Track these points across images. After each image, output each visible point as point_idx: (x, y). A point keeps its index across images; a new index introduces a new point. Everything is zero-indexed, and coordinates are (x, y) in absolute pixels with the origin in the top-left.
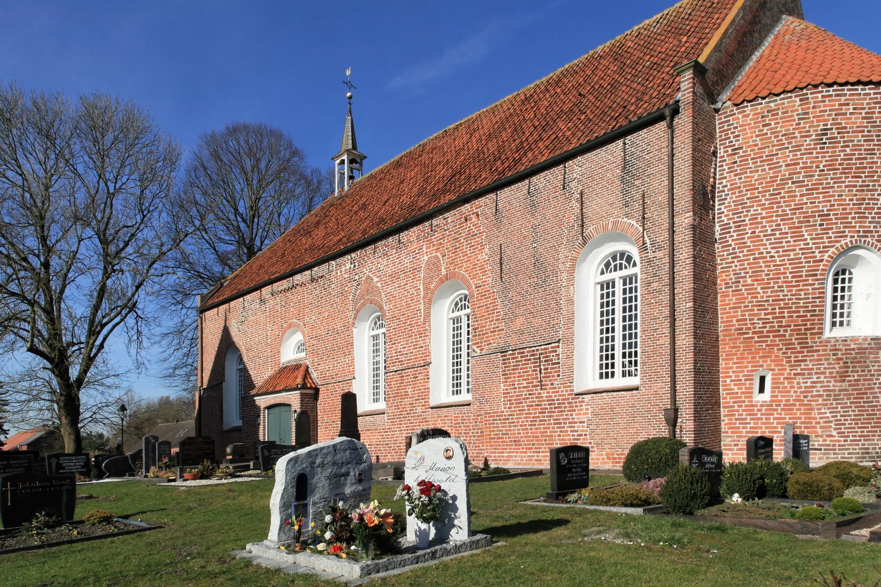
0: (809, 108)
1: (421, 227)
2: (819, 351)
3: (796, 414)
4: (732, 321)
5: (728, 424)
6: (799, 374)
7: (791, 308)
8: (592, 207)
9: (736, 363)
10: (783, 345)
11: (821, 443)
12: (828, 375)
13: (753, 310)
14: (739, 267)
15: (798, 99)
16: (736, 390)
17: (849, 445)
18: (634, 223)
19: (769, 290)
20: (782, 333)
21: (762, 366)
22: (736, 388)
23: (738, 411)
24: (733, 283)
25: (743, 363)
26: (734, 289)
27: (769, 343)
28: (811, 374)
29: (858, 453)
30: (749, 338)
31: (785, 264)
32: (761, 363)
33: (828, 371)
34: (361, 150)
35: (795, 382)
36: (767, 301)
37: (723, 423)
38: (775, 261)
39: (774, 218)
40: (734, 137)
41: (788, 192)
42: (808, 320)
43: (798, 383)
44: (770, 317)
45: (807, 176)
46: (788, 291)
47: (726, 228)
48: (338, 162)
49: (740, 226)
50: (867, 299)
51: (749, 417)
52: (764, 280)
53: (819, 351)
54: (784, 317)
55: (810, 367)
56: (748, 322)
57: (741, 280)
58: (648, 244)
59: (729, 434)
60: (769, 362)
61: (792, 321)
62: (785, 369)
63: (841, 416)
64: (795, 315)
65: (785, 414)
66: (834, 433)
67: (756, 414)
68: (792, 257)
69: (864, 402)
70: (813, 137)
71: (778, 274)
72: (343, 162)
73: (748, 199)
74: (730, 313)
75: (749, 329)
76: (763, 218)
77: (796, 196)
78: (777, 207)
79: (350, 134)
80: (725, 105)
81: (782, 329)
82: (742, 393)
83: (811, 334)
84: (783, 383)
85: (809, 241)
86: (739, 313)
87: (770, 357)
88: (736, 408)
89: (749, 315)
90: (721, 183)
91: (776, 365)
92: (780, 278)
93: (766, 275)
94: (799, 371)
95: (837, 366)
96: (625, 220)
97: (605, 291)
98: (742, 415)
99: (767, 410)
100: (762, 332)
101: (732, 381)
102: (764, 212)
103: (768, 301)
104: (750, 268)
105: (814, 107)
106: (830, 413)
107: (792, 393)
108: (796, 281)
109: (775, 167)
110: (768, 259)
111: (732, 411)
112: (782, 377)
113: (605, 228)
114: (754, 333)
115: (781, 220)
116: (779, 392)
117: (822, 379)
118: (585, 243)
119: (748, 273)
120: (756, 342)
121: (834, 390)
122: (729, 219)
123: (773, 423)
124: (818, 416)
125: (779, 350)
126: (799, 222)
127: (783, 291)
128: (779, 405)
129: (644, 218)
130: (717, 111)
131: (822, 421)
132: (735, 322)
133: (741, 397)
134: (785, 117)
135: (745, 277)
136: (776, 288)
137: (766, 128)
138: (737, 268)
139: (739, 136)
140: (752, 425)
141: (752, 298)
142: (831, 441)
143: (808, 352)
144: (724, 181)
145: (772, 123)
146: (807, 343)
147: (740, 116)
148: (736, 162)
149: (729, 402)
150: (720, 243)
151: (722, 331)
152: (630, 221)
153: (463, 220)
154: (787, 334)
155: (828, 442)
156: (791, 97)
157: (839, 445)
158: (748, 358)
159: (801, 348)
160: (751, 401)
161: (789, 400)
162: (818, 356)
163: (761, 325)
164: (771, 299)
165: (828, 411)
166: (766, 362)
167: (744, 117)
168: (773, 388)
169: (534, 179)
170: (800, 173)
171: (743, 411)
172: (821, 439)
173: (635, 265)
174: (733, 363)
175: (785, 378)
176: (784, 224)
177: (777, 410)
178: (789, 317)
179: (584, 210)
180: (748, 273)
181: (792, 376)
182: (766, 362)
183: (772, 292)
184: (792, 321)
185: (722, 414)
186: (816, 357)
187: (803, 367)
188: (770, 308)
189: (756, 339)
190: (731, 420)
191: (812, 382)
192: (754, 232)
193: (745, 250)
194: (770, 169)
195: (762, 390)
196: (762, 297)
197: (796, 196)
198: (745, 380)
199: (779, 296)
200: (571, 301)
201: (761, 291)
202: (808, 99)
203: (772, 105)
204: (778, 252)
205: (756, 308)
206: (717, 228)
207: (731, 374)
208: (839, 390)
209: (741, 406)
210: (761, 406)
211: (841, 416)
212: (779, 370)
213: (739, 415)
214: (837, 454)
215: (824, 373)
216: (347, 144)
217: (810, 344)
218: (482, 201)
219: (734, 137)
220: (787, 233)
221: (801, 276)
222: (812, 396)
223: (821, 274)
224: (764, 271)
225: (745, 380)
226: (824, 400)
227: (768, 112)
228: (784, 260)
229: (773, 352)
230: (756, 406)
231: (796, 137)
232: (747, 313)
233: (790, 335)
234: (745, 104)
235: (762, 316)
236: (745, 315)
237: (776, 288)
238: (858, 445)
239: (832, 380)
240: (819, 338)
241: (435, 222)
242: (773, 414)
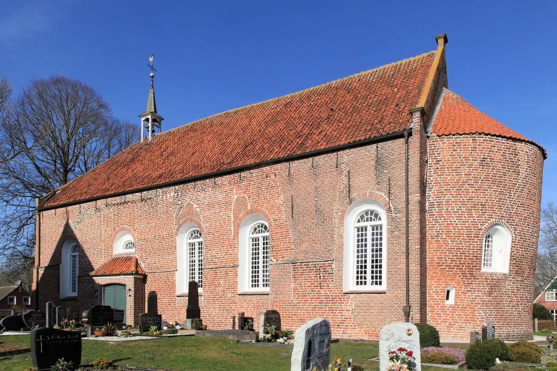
0: (476, 145)
1: (232, 176)
5: (431, 316)
6: (469, 291)
8: (355, 182)
10: (462, 274)
15: (471, 139)
18: (383, 195)
21: (450, 285)
23: (436, 309)
34: (160, 113)
37: (428, 316)
38: (458, 227)
39: (458, 203)
40: (437, 154)
41: (465, 189)
43: (469, 296)
45: (475, 182)
47: (432, 205)
48: (144, 119)
49: (440, 205)
50: (500, 252)
54: (462, 259)
58: (392, 208)
61: (466, 261)
62: (462, 288)
70: (478, 161)
72: (147, 120)
73: (444, 190)
75: (444, 263)
76: (452, 202)
77: (469, 192)
78: (460, 197)
79: (153, 101)
80: (432, 135)
82: (439, 299)
83: (476, 269)
84: (461, 295)
85: (475, 218)
90: (430, 179)
91: (458, 285)
93: (454, 234)
94: (469, 289)
96: (378, 192)
97: (360, 233)
100: (451, 266)
102: (453, 199)
105: (479, 145)
108: (469, 239)
109: (459, 174)
113: (364, 195)
114: (446, 266)
115: (462, 204)
118: (351, 202)
120: (447, 271)
122: (434, 200)
126: (471, 207)
128: (459, 307)
129: (390, 193)
130: (428, 137)
132: (436, 259)
133: (438, 302)
134: (465, 148)
137: (455, 152)
139: (440, 154)
143: (474, 279)
144: (431, 178)
145: (458, 150)
147: (441, 143)
148: (438, 168)
150: (429, 213)
151: (429, 263)
152: (381, 193)
153: (264, 176)
156: (468, 137)
158: (442, 280)
161: (463, 305)
167: (443, 143)
169: (316, 158)
170: (472, 180)
171: (439, 309)
173: (380, 219)
176: (463, 207)
179: (351, 183)
184: (466, 261)
185: (428, 310)
189: (447, 269)
190: (432, 314)
192: (447, 209)
193: (442, 218)
194: (456, 175)
196: (451, 246)
197: (469, 192)
200: (341, 237)
202: (476, 140)
203: (458, 139)
204: (460, 222)
206: (427, 204)
209: (438, 307)
210: (450, 307)
216: (150, 108)
218: (279, 166)
219: (437, 154)
220: (465, 212)
221: (471, 237)
223: (481, 237)
227: (456, 143)
231: (470, 160)
233: (465, 269)
234: (444, 136)
235: (451, 257)
241: (243, 174)
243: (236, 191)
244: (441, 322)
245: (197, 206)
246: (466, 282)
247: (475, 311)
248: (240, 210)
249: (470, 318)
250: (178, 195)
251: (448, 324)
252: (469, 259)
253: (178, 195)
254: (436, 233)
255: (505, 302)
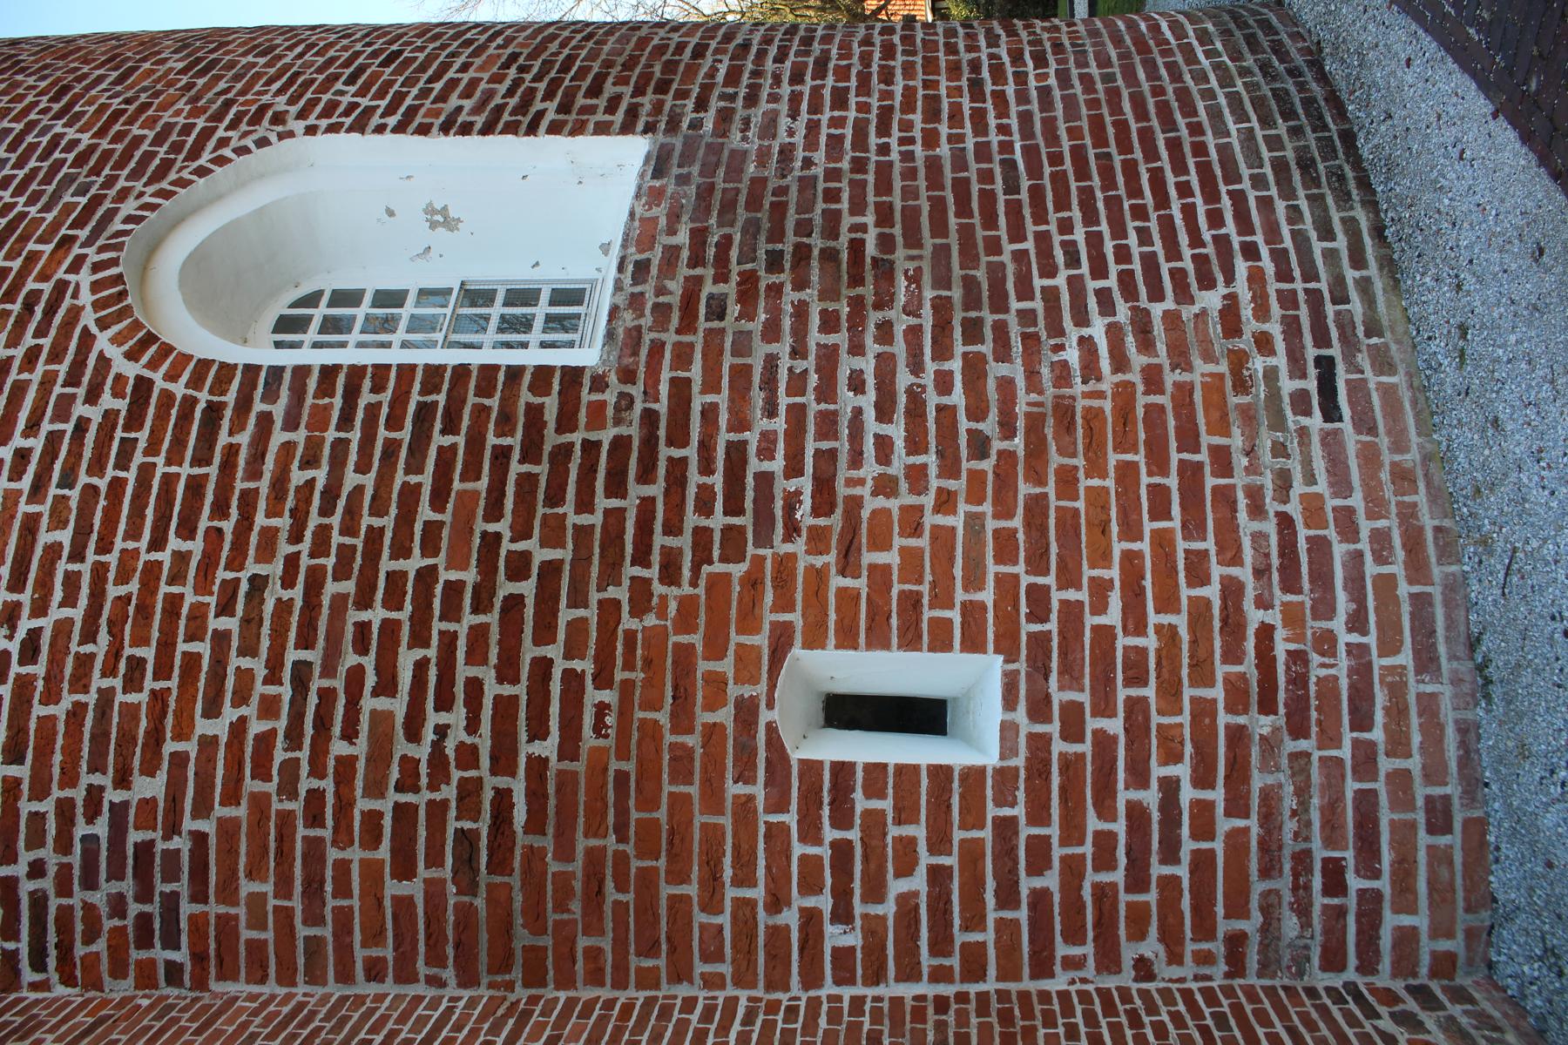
2: (681, 388)
3: (1097, 499)
4: (404, 905)
7: (375, 535)
9: (712, 883)
10: (611, 574)
11: (1281, 361)
12: (841, 338)
13: (346, 766)
14: (47, 853)
16: (918, 882)
17: (1273, 234)
19: (235, 662)
20: (527, 588)
21: (747, 712)
22: (897, 887)
23: (1072, 869)
24: (144, 895)
25: (713, 836)
26: (183, 886)
27: (585, 666)
28: (828, 424)
29: (1316, 200)
30: (536, 795)
31: (99, 571)
32: (725, 716)
33: (815, 337)
35: (871, 504)
36: (301, 674)
38: (63, 627)
42: (475, 442)
43: (885, 486)
44: (406, 660)
46: (267, 550)
51: (1123, 796)
52: (158, 697)
53: (681, 388)
54: (427, 576)
55: (780, 424)
56: (421, 799)
57: (134, 837)
59: (1251, 925)
60: (727, 666)
62: (785, 565)
63: (1099, 271)
64: (425, 513)
65: (1102, 557)
66: (1212, 300)
67: (1104, 743)
68: (65, 537)
69: (1012, 187)
71: (144, 611)
74: (343, 920)
75: (470, 791)
81: (505, 588)
82: (939, 842)
83: (566, 422)
84: (880, 576)
86: (355, 854)
87: (685, 656)
88: (1051, 880)
89: (376, 788)
91: (749, 622)
92: (174, 602)
94: (805, 484)
95: (790, 296)
98: (1105, 842)
99: (1070, 675)
100: (505, 706)
101: (842, 915)
103: (301, 674)
104: (69, 779)
106: (1082, 319)
107: (957, 521)
110: (39, 669)
111: (1073, 905)
112: (837, 582)
114: (503, 760)
116: (943, 598)
117: (868, 365)
119: (95, 794)
120: (569, 748)
121: (942, 308)
123: (1168, 635)
124: (1109, 380)
125: (641, 597)
127: (258, 583)
128: (1039, 597)
131: (1138, 360)
132: (414, 889)
133: (971, 853)
135: (119, 810)
136: (231, 624)
138: (52, 860)
140: (1183, 771)
141: (262, 773)
142: (1262, 312)
143: (679, 436)
146: (620, 444)
149: (1007, 929)
154: (541, 555)
155: (1275, 329)
157: (1284, 275)
159: (646, 476)
160: (1005, 777)
161: (1005, 544)
162: (711, 385)
163: (457, 717)
164: (292, 655)
165: (1073, 333)
166: (717, 683)
168: (910, 641)
171: (1072, 832)
172: (1258, 364)
174: (712, 902)
175: (848, 564)
177: (1071, 612)
178: (430, 547)
180: (95, 794)
181: (836, 521)
182: (717, 683)
183: (249, 650)
186: (722, 399)
187: (777, 465)
188: (351, 659)
189: (548, 748)
191: (884, 414)
195: (924, 716)
196: (269, 707)
198: (842, 818)
199: (283, 607)
201: (230, 714)
205: (339, 748)
207: (790, 918)
208: (942, 281)
209: (1039, 849)
210: (1040, 709)
211: (1099, 271)
212: (784, 603)
213: (1104, 860)
214: (1338, 282)
215: (828, 357)
217: (634, 431)
222: (977, 411)
224: (106, 696)
225: (842, 818)
226: (1003, 354)
228: (72, 581)
229: (656, 638)
230: (1039, 744)
232: (362, 804)
233: (554, 535)
235: (398, 706)
236: (373, 818)
237: (231, 624)
238: (1266, 204)
239: (874, 317)
240: (599, 383)
242: (1104, 635)
244: (1236, 807)
246: (718, 520)
247: (1064, 412)
249: (1158, 463)
251: (1262, 725)
252: (439, 498)
254: (108, 888)
255: (944, 150)
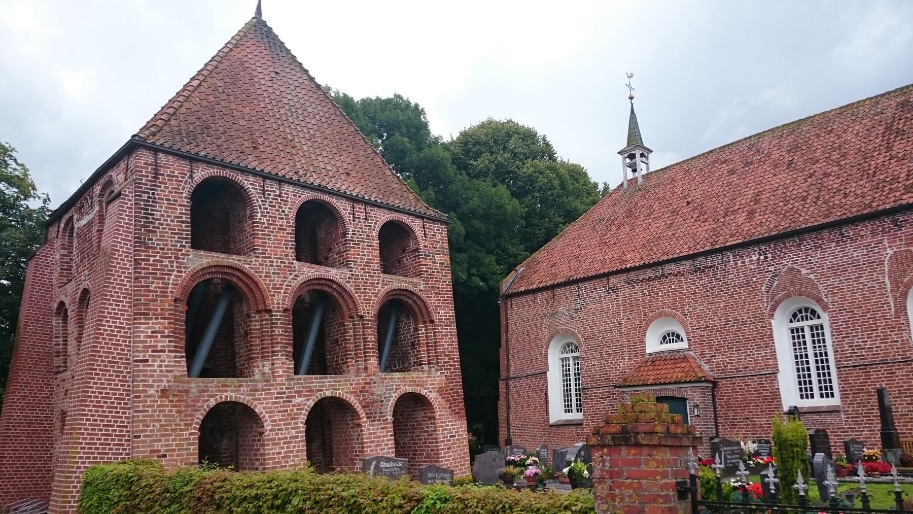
243: (889, 243)
245: (809, 271)
248: (904, 271)
250: (766, 258)
253: (766, 258)
